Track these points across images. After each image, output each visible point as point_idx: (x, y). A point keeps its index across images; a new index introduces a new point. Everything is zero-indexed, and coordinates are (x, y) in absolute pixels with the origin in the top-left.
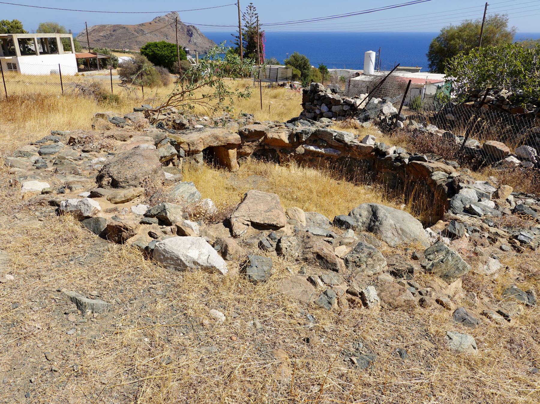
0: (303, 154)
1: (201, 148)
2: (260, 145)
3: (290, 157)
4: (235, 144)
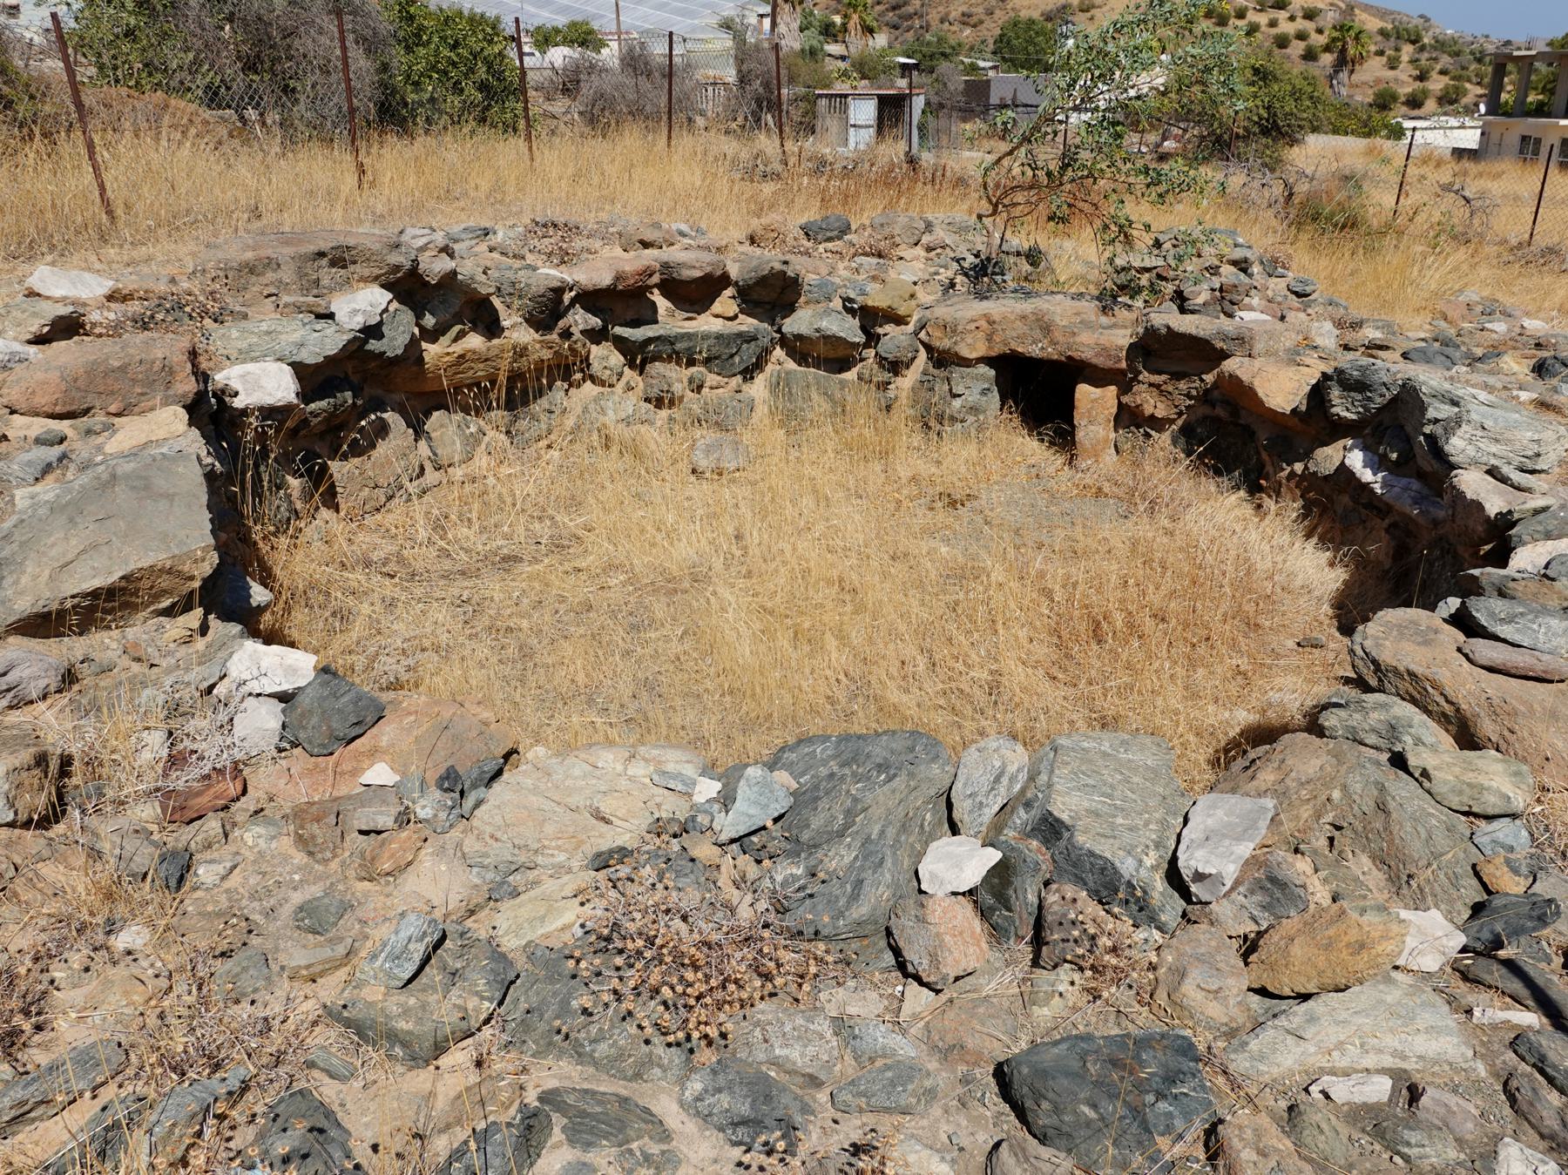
1: (973, 347)
2: (1206, 397)
4: (1095, 366)
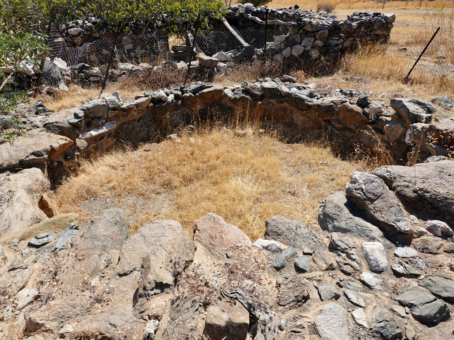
0: (87, 147)
3: (78, 159)
